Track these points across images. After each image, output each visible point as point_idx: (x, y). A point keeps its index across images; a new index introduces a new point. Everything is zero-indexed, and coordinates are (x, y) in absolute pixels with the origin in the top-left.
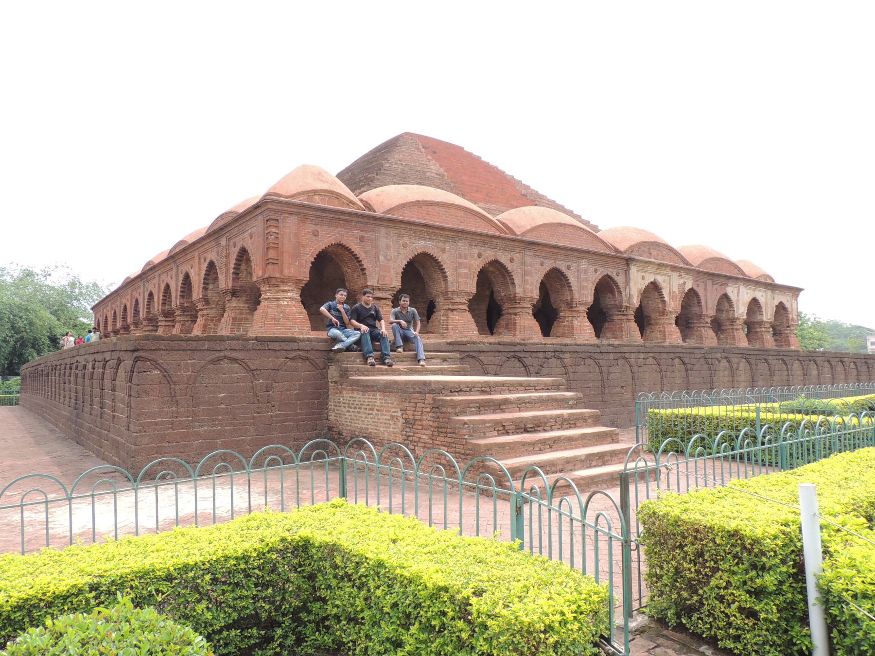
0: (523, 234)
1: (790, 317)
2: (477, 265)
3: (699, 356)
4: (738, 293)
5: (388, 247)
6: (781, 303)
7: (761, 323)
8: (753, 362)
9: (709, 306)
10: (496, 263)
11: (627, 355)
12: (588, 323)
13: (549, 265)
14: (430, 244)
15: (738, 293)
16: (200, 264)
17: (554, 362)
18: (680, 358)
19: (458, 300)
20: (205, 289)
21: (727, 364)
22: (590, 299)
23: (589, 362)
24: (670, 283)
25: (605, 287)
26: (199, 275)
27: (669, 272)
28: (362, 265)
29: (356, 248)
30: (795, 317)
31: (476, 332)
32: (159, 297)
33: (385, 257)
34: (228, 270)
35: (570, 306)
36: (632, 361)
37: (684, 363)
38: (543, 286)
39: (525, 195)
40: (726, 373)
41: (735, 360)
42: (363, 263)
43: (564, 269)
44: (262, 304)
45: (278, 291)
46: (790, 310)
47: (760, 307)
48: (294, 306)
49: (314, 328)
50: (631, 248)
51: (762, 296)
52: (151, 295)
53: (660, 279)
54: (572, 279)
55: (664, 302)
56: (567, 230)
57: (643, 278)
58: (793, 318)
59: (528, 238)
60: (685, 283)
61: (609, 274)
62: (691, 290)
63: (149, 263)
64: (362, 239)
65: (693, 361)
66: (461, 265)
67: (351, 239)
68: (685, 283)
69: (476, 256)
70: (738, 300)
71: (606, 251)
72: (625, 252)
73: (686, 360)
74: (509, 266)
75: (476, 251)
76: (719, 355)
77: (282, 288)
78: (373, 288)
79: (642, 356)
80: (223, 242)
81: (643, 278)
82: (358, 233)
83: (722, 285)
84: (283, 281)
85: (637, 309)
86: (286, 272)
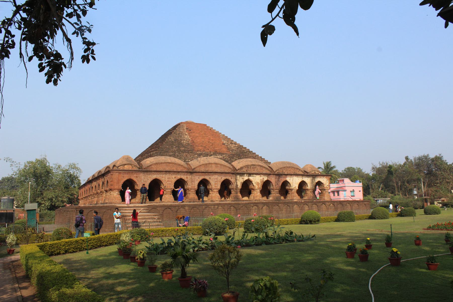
0: (194, 168)
1: (325, 186)
2: (174, 180)
7: (308, 190)
8: (270, 206)
10: (181, 179)
13: (201, 178)
14: (158, 176)
17: (182, 209)
21: (257, 208)
22: (219, 187)
23: (195, 209)
27: (255, 175)
29: (135, 179)
31: (173, 200)
36: (213, 208)
39: (224, 144)
40: (256, 210)
41: (260, 206)
46: (325, 183)
47: (307, 184)
49: (123, 201)
50: (242, 168)
51: (308, 180)
53: (251, 178)
54: (211, 181)
56: (213, 165)
57: (243, 179)
59: (197, 170)
60: (263, 179)
63: (94, 175)
64: (137, 177)
65: (240, 207)
67: (134, 177)
68: (263, 179)
71: (230, 171)
72: (239, 169)
73: (236, 206)
75: (174, 176)
79: (216, 206)
80: (105, 177)
81: (243, 179)
82: (135, 175)
84: (115, 190)
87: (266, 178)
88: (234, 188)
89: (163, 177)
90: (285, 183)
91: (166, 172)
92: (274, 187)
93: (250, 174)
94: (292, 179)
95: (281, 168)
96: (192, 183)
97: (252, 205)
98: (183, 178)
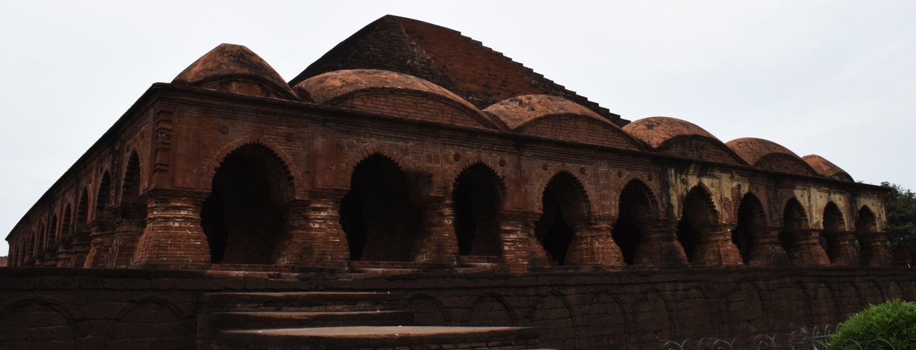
0: (520, 129)
4: (809, 197)
6: (865, 208)
9: (773, 217)
10: (479, 168)
12: (614, 245)
13: (555, 167)
15: (809, 197)
16: (97, 177)
20: (100, 208)
22: (614, 212)
24: (720, 188)
25: (634, 195)
26: (95, 192)
27: (717, 173)
28: (289, 172)
29: (281, 149)
32: (60, 221)
34: (119, 182)
35: (589, 222)
38: (548, 197)
42: (290, 169)
43: (576, 174)
44: (150, 226)
45: (167, 209)
47: (840, 214)
48: (190, 229)
50: (667, 144)
51: (840, 201)
52: (55, 219)
53: (706, 182)
55: (715, 212)
56: (580, 124)
60: (739, 187)
61: (638, 177)
62: (749, 195)
64: (289, 138)
69: (451, 158)
70: (810, 206)
74: (499, 170)
75: (452, 152)
77: (173, 204)
81: (684, 182)
82: (283, 129)
85: (680, 222)
86: (179, 182)
88: (662, 217)
89: (406, 152)
90: (794, 208)
91: (422, 125)
92: (768, 219)
93: (705, 169)
96: (532, 183)
98: (489, 164)
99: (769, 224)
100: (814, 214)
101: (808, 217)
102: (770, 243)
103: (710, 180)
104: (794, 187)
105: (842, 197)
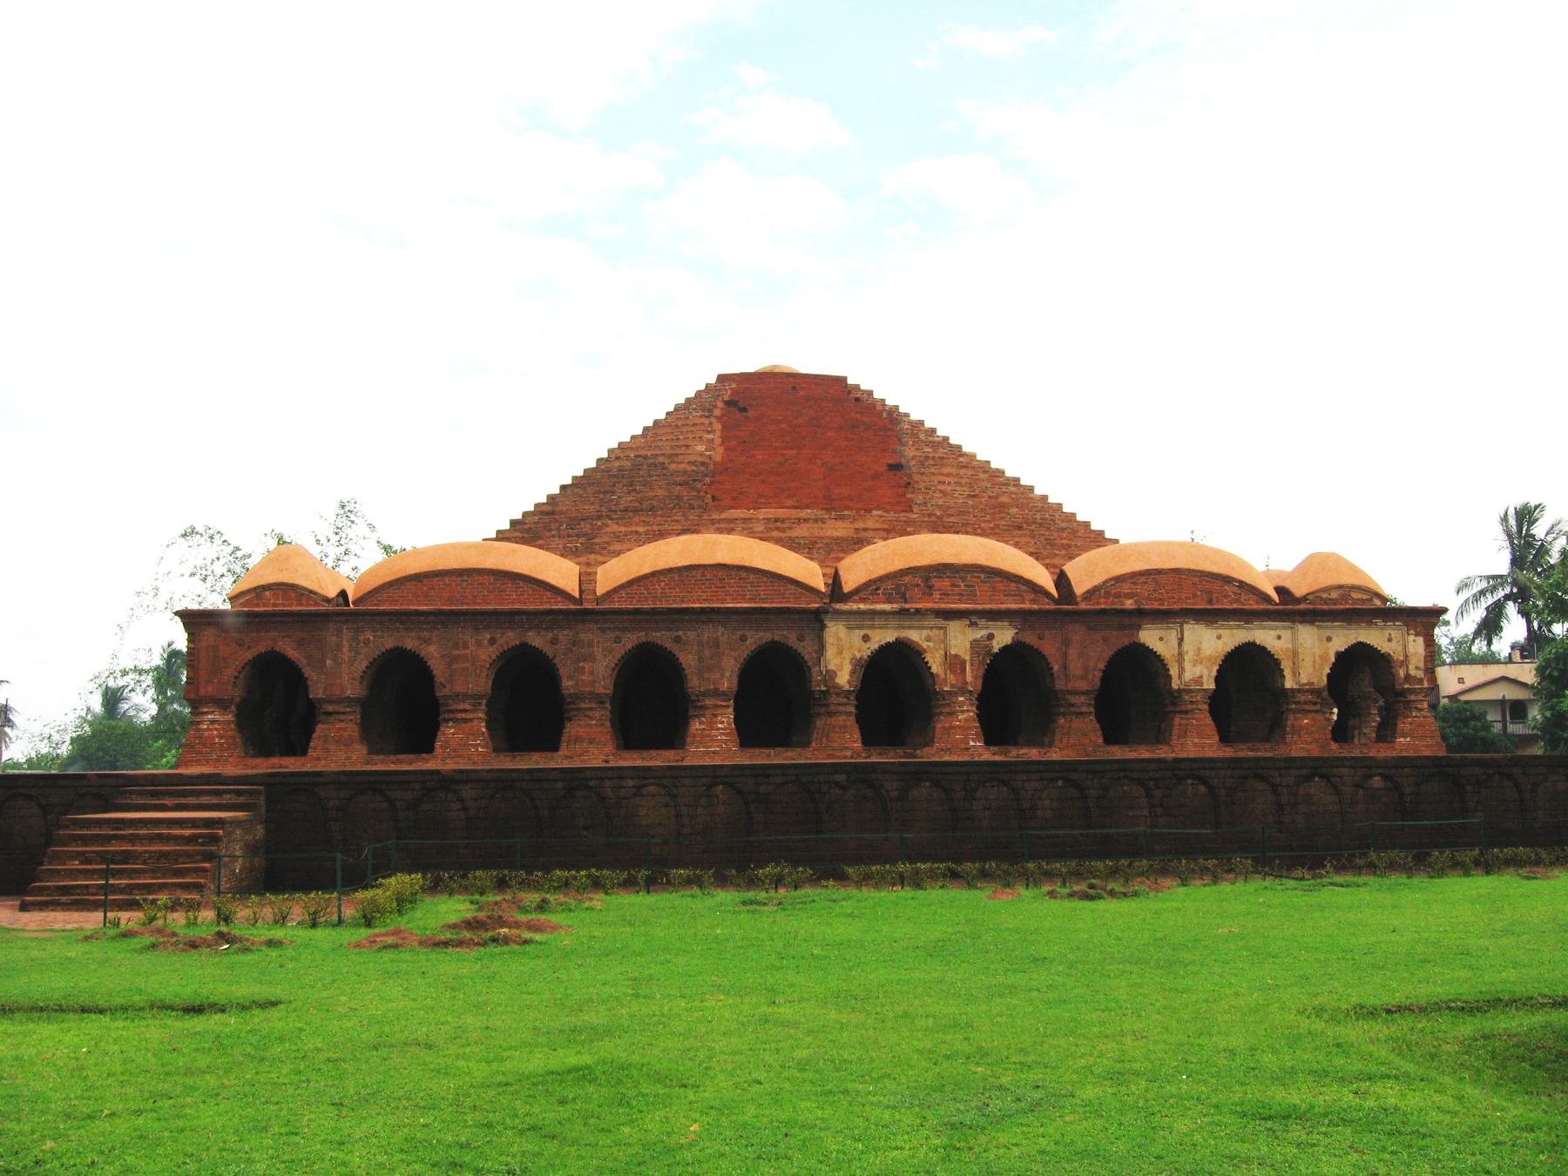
1: (1402, 673)
3: (780, 780)
4: (1181, 640)
5: (339, 647)
10: (524, 645)
11: (591, 783)
13: (631, 640)
18: (728, 784)
19: (455, 707)
24: (944, 641)
27: (941, 622)
30: (1420, 674)
33: (335, 660)
37: (740, 792)
41: (891, 787)
43: (669, 645)
47: (1277, 663)
53: (915, 636)
54: (688, 660)
57: (866, 638)
58: (1408, 677)
61: (776, 639)
64: (300, 643)
65: (762, 789)
66: (456, 659)
68: (991, 637)
70: (1181, 655)
74: (548, 650)
76: (842, 778)
78: (319, 700)
81: (866, 638)
83: (1121, 628)
87: (1004, 636)
89: (429, 641)
94: (1173, 636)
95: (1119, 579)
97: (842, 778)
99: (1059, 685)
100: (1187, 665)
101: (1174, 672)
102: (1064, 714)
103: (925, 633)
104: (1139, 628)
105: (1286, 634)
